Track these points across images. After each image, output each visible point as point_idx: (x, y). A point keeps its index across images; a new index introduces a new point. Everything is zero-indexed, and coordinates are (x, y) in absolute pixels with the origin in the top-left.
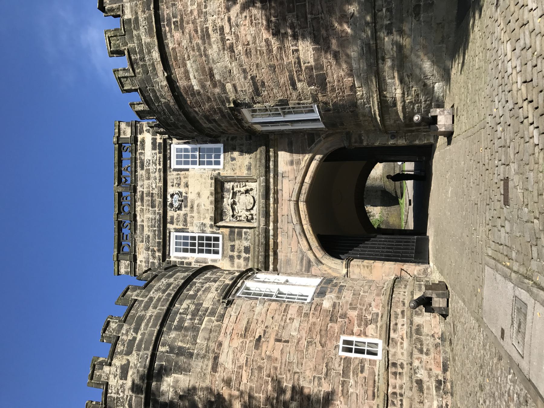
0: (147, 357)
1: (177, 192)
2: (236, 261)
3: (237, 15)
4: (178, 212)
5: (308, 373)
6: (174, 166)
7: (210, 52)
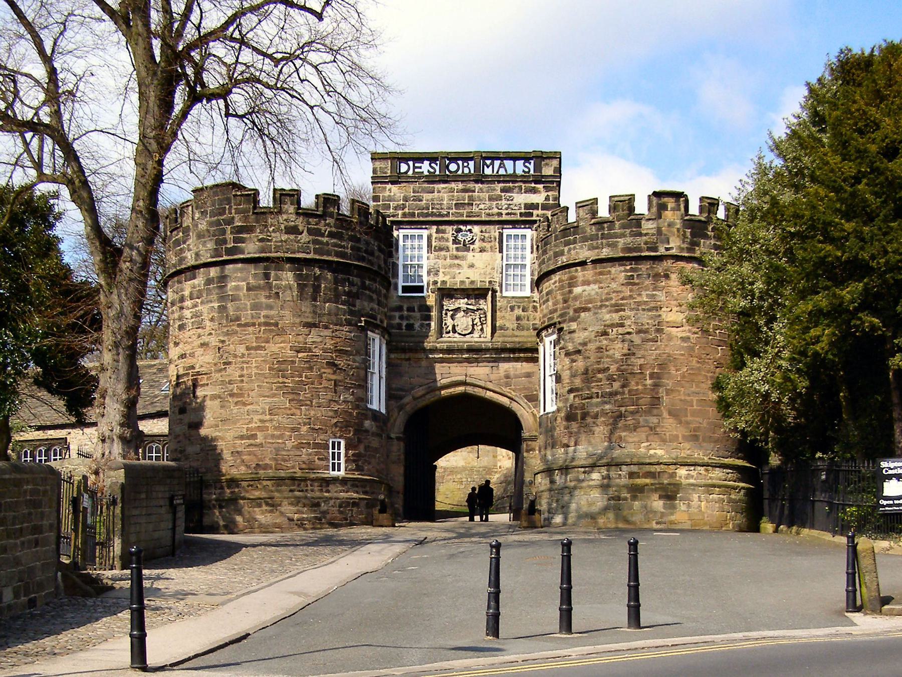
0: (308, 253)
1: (475, 238)
2: (397, 314)
3: (632, 342)
4: (451, 239)
5: (312, 413)
6: (506, 232)
7: (604, 310)
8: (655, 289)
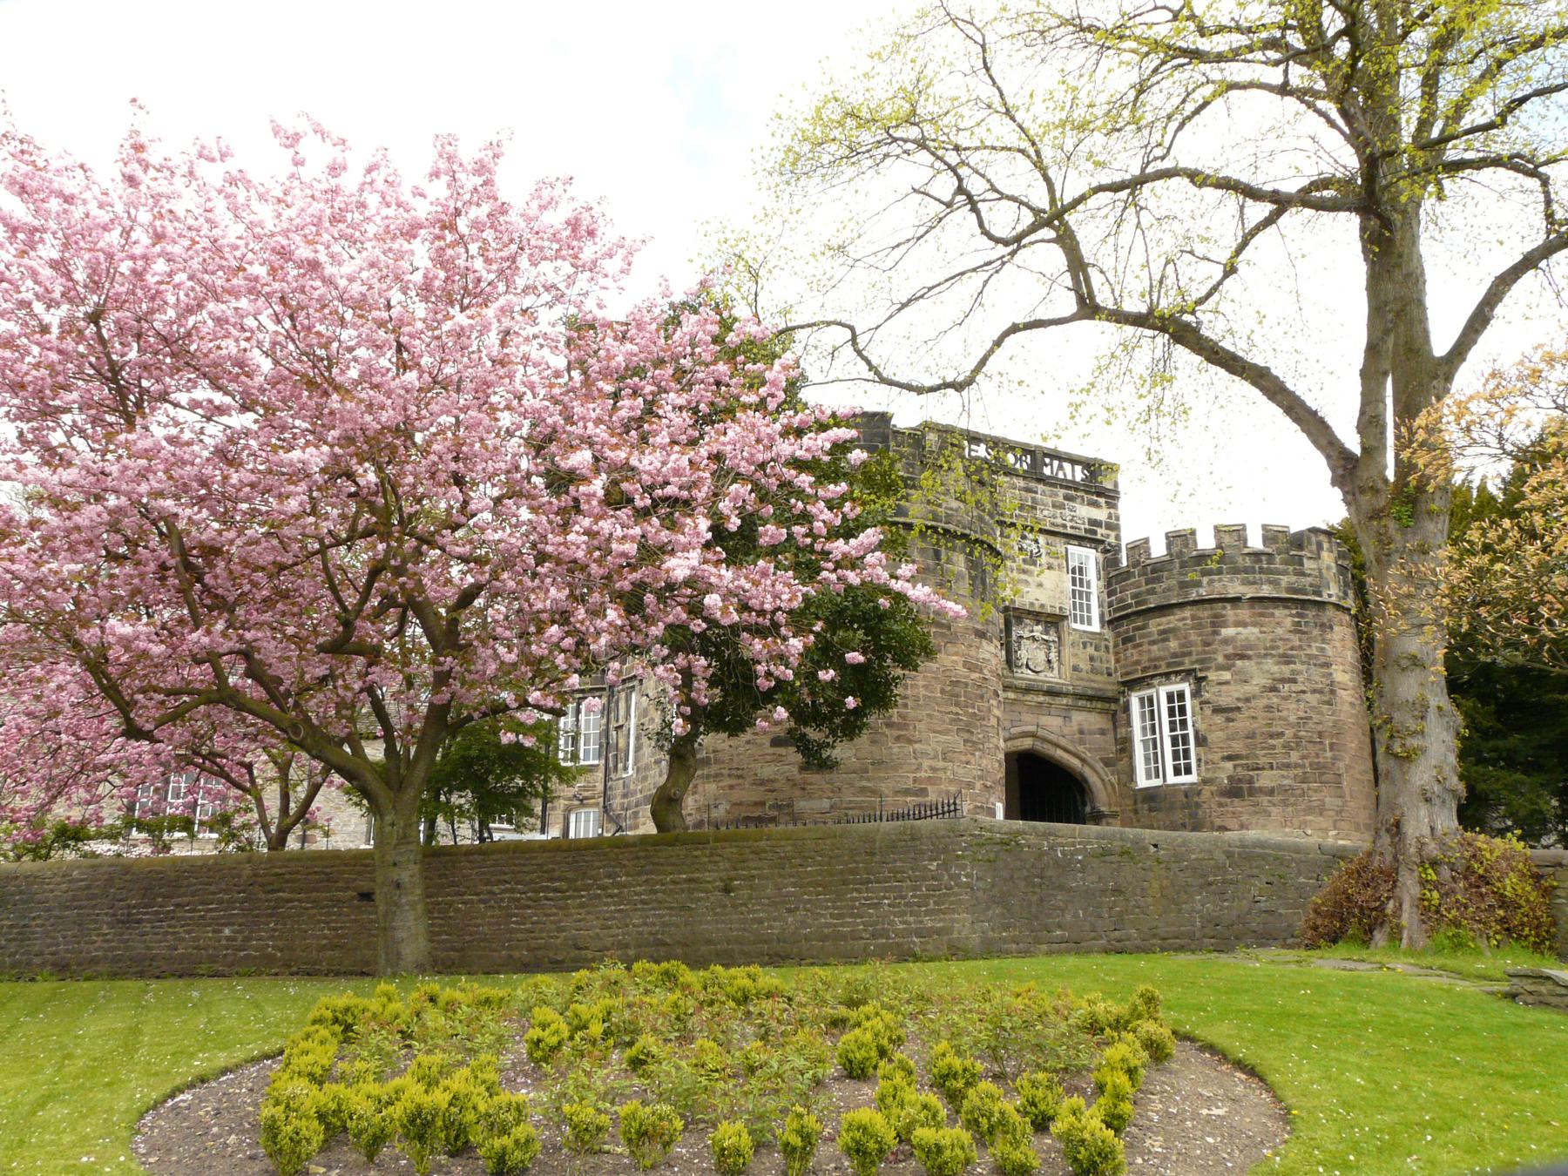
8: (1323, 641)
